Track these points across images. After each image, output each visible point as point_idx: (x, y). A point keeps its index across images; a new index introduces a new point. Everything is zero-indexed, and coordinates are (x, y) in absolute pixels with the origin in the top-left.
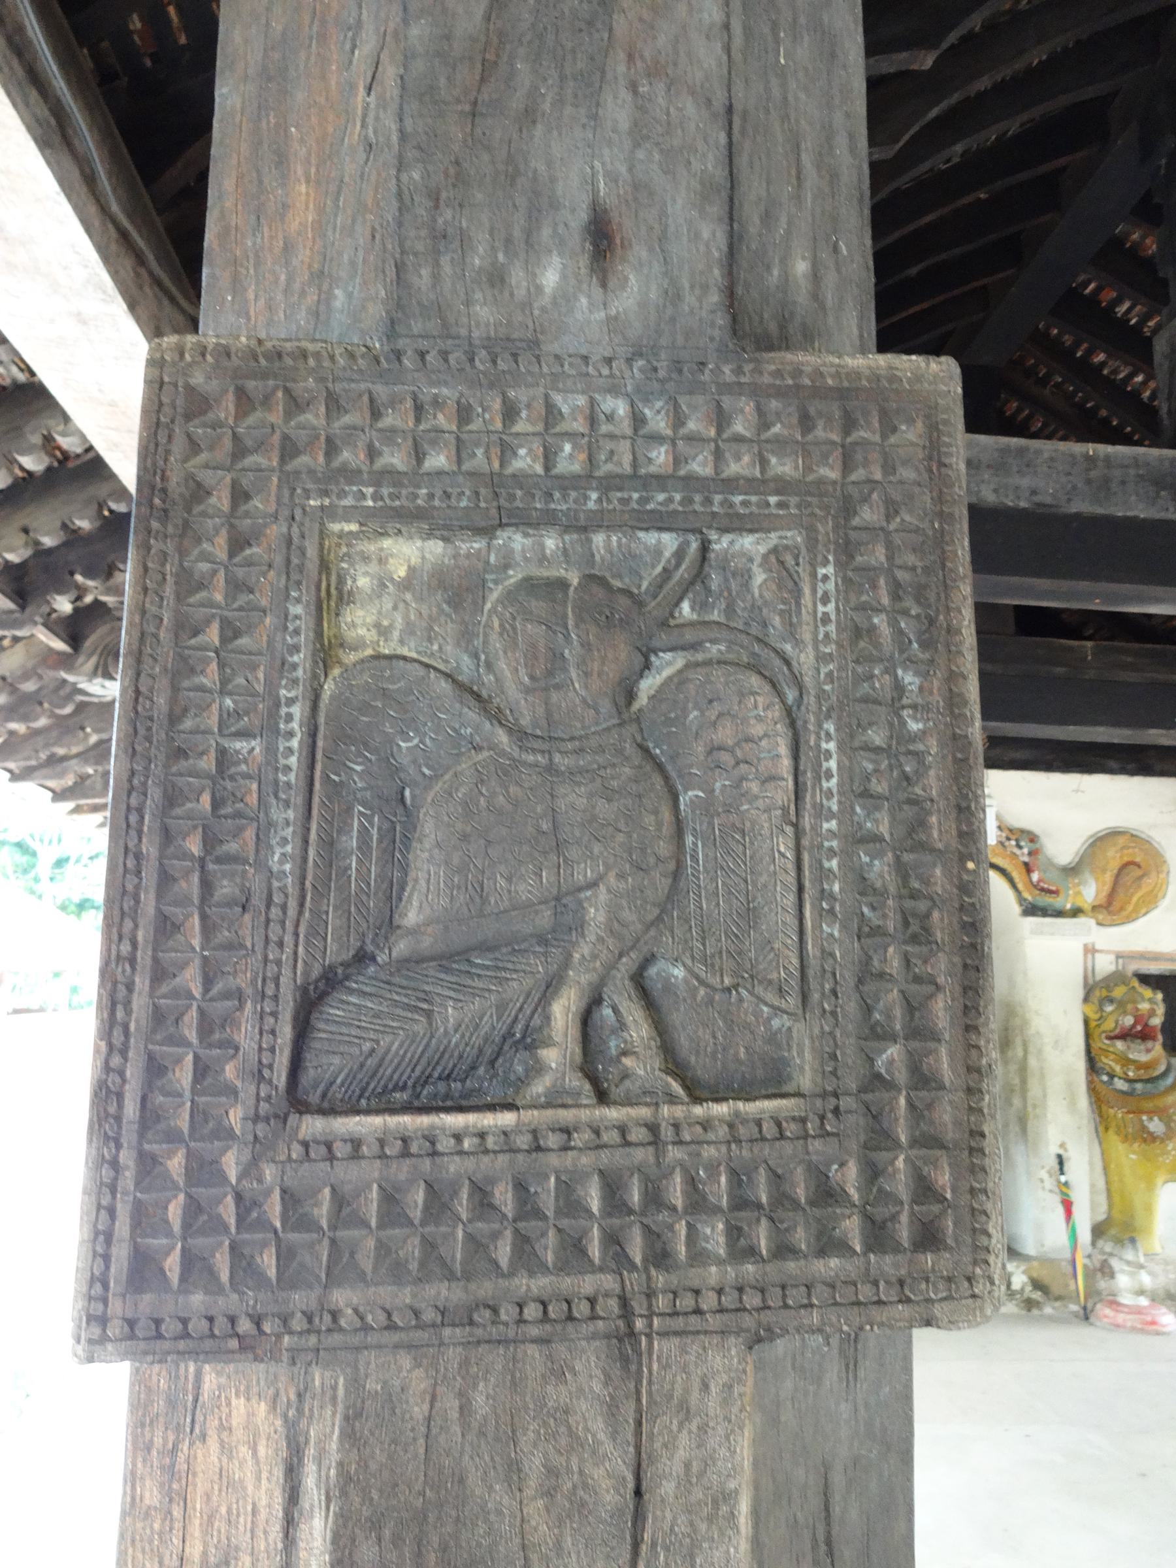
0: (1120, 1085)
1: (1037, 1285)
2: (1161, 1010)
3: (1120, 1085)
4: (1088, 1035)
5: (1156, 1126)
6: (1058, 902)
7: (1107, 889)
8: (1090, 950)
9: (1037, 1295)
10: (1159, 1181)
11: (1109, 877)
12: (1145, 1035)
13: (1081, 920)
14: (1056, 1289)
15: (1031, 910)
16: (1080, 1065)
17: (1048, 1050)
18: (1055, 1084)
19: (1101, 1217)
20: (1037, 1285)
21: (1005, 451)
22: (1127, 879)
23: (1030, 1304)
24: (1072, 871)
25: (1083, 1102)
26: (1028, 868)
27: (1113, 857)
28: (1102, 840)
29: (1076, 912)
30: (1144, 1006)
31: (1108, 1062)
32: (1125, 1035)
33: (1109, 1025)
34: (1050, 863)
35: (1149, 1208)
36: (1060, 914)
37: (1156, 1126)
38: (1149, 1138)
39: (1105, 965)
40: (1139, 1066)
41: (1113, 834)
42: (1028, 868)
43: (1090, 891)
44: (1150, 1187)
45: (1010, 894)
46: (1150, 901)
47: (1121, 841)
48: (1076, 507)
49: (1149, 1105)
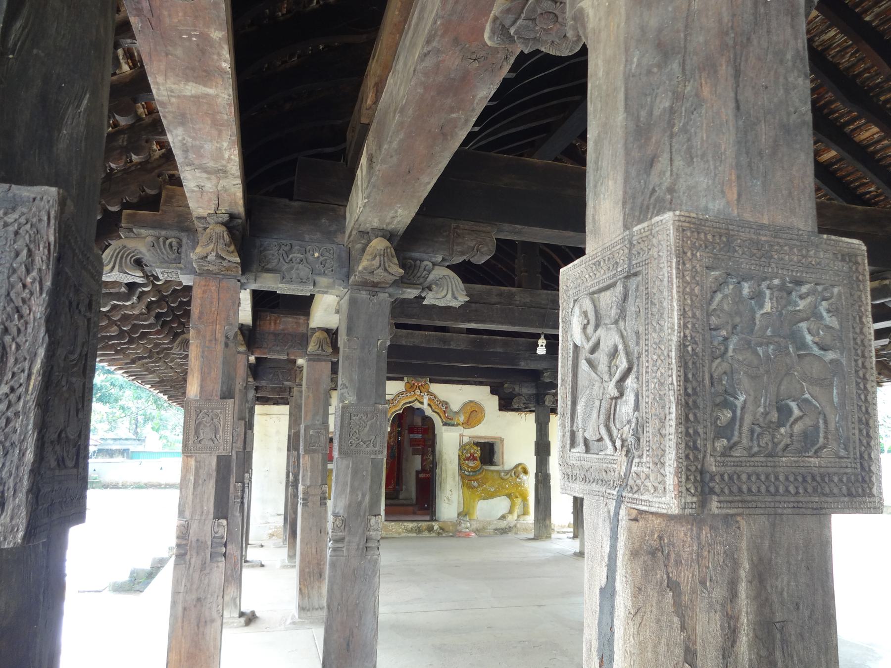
0: (467, 473)
1: (441, 528)
2: (479, 453)
3: (467, 473)
4: (460, 459)
5: (475, 484)
6: (452, 422)
7: (467, 418)
8: (461, 436)
9: (441, 531)
10: (477, 500)
11: (467, 415)
12: (474, 459)
13: (459, 427)
14: (446, 530)
15: (445, 424)
16: (457, 468)
17: (448, 464)
18: (450, 473)
19: (461, 510)
20: (441, 528)
21: (408, 333)
22: (473, 415)
23: (439, 533)
24: (457, 413)
25: (457, 478)
26: (445, 412)
27: (469, 409)
28: (466, 405)
29: (458, 425)
30: (472, 451)
31: (464, 467)
32: (468, 459)
33: (464, 457)
34: (451, 410)
35: (473, 507)
36: (453, 425)
37: (475, 484)
38: (474, 487)
39: (466, 440)
40: (474, 468)
41: (470, 402)
42: (445, 412)
43: (462, 419)
44: (474, 502)
45: (440, 419)
46: (479, 422)
47: (472, 404)
48: (423, 345)
49: (473, 478)
